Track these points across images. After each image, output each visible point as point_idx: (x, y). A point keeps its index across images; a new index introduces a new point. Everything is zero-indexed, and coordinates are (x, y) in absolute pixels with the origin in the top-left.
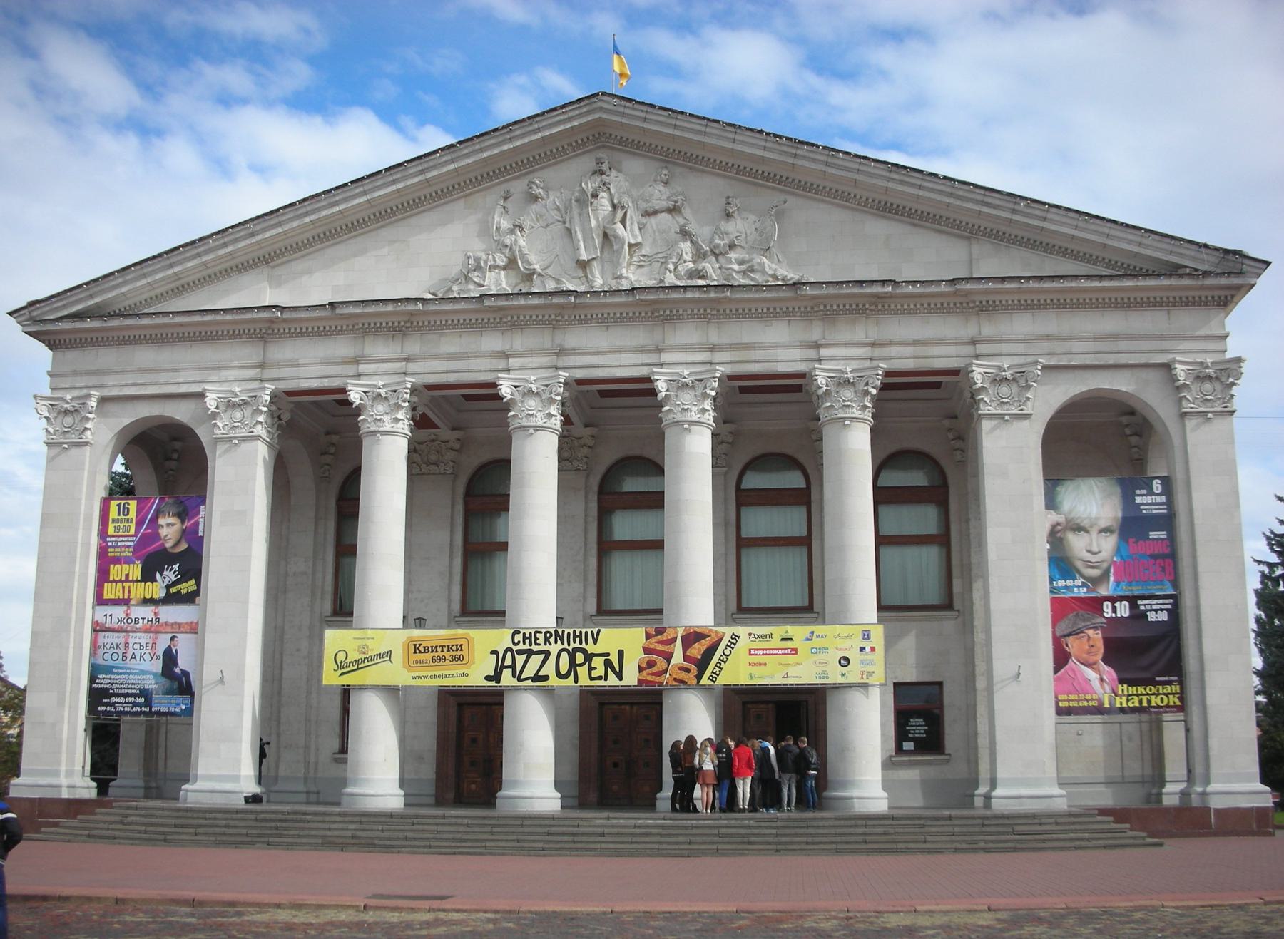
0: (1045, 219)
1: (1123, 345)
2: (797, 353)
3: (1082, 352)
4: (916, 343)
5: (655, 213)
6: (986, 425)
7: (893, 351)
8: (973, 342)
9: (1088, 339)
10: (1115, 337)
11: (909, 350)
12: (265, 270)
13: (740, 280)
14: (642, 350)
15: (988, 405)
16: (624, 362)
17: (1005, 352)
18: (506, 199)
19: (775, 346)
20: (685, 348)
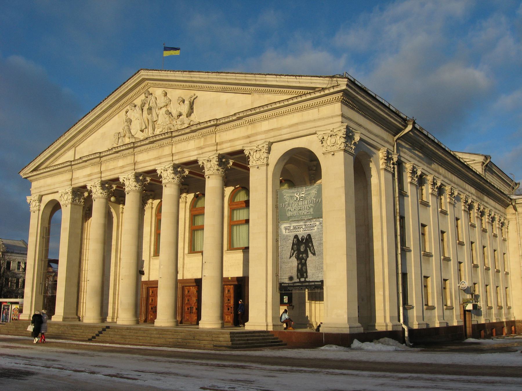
0: (266, 81)
1: (300, 127)
2: (196, 153)
3: (285, 133)
4: (230, 141)
5: (161, 108)
6: (251, 170)
7: (224, 146)
8: (248, 137)
9: (286, 128)
10: (297, 124)
11: (228, 145)
12: (74, 149)
13: (179, 127)
14: (155, 159)
15: (252, 163)
16: (151, 164)
17: (258, 139)
18: (127, 112)
19: (189, 151)
20: (165, 156)
